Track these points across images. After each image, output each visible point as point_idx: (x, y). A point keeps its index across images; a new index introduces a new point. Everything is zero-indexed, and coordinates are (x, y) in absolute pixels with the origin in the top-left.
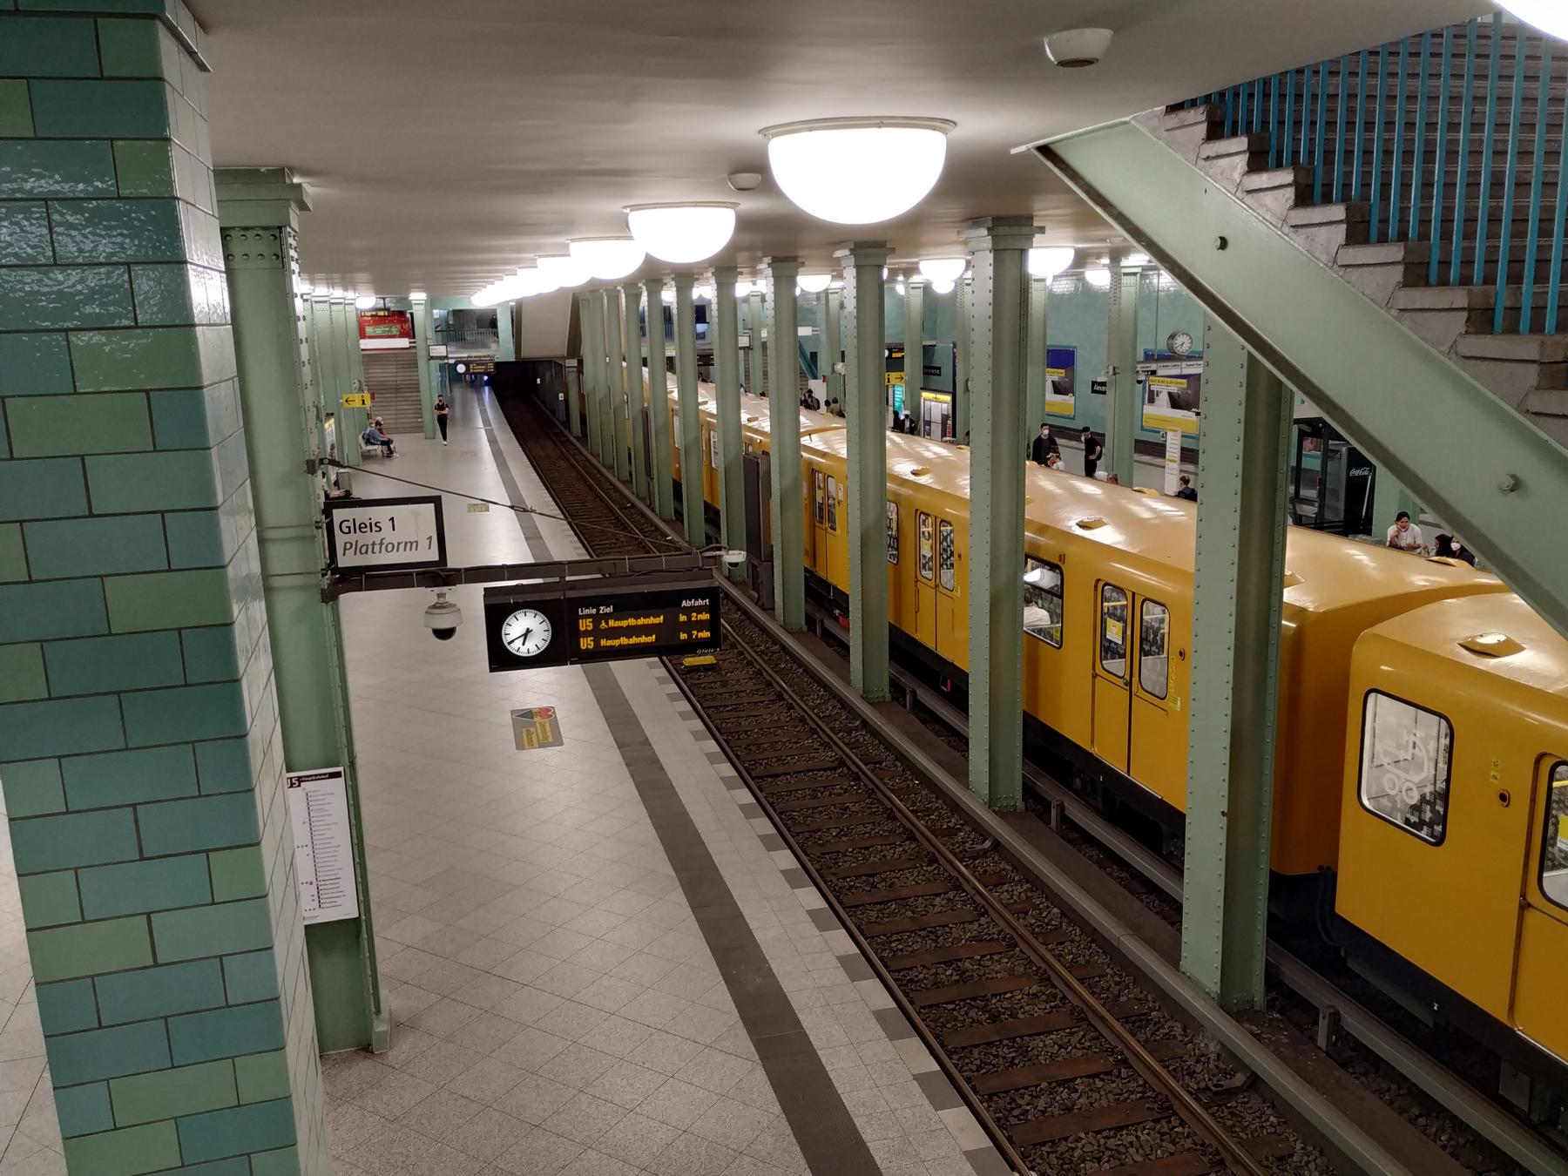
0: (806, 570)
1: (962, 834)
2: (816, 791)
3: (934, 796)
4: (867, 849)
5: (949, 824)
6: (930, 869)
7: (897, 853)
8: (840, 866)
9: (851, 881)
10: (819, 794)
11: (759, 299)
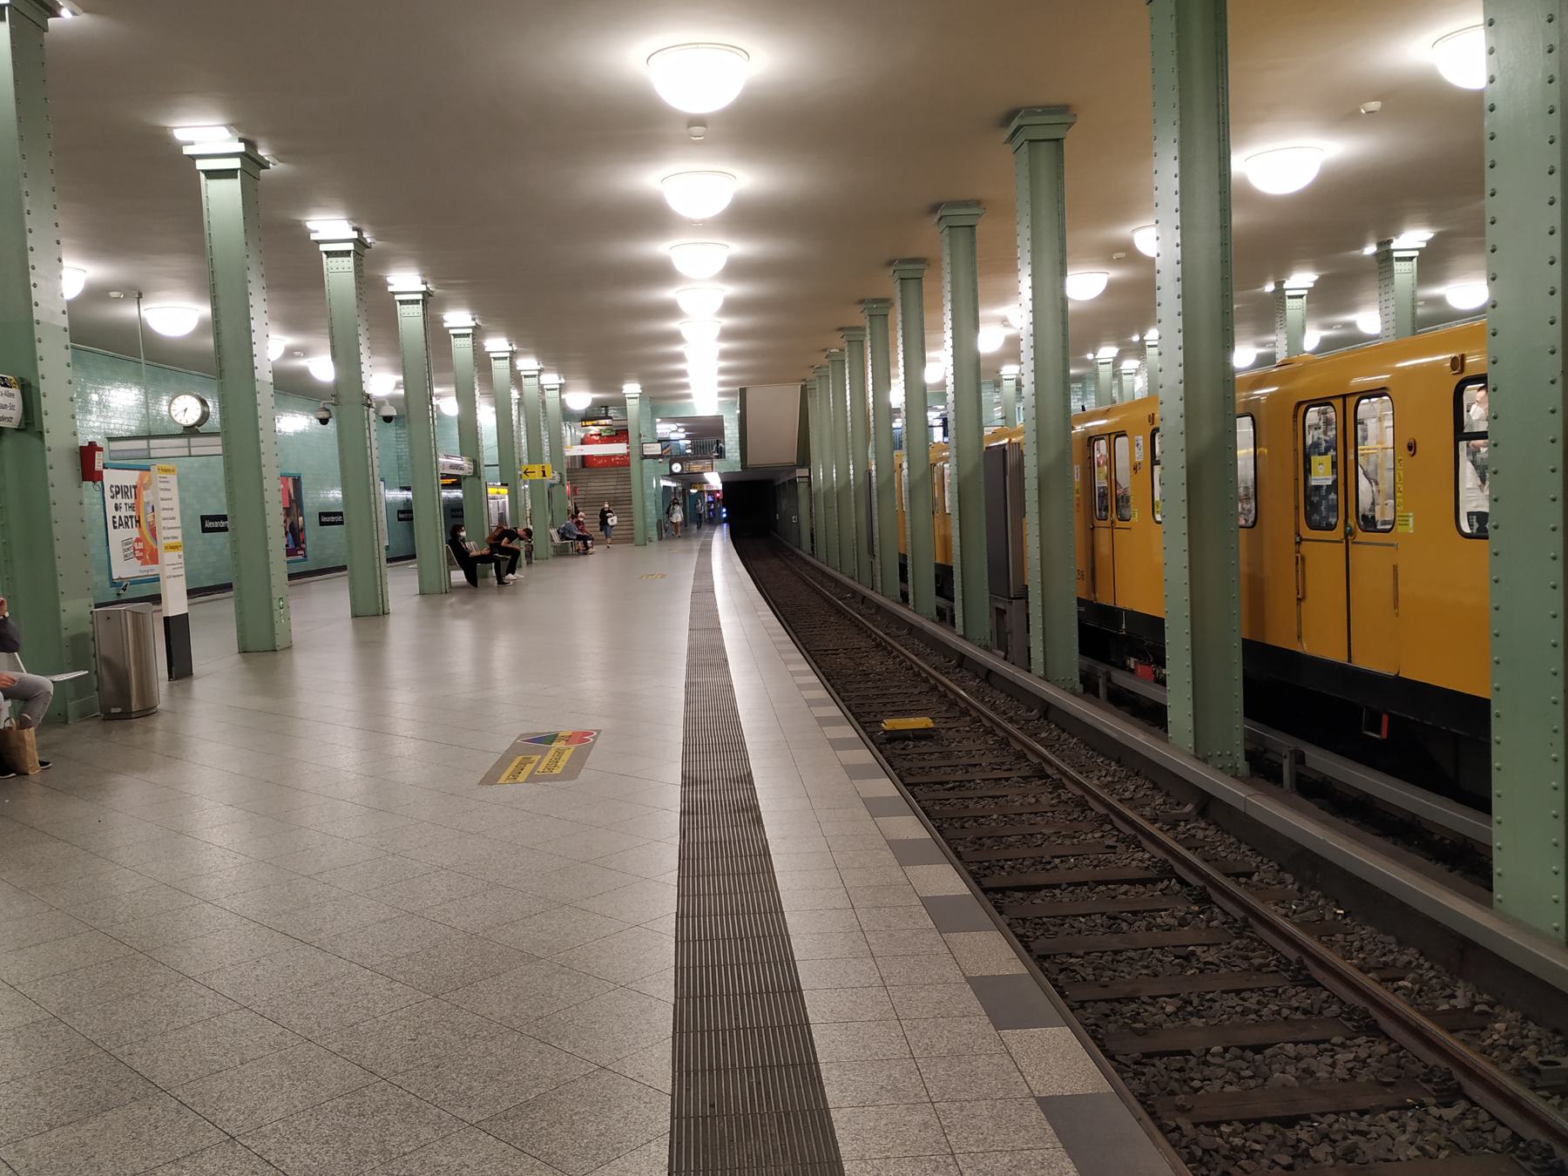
0: (1080, 602)
1: (1500, 1026)
2: (1115, 918)
3: (1391, 939)
4: (1258, 1049)
5: (1453, 1002)
6: (1449, 1113)
7: (1340, 1065)
8: (1197, 1090)
9: (1234, 1134)
10: (1124, 926)
11: (1013, 382)
